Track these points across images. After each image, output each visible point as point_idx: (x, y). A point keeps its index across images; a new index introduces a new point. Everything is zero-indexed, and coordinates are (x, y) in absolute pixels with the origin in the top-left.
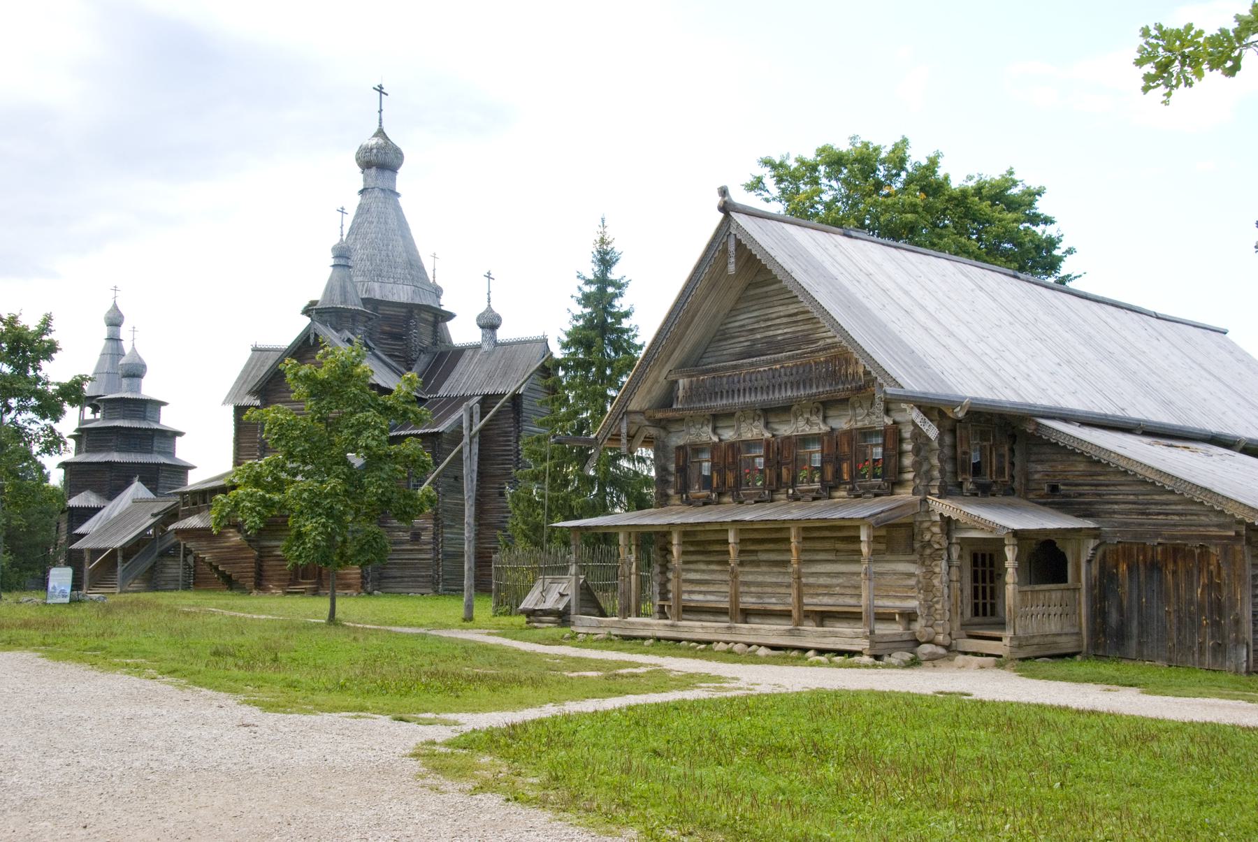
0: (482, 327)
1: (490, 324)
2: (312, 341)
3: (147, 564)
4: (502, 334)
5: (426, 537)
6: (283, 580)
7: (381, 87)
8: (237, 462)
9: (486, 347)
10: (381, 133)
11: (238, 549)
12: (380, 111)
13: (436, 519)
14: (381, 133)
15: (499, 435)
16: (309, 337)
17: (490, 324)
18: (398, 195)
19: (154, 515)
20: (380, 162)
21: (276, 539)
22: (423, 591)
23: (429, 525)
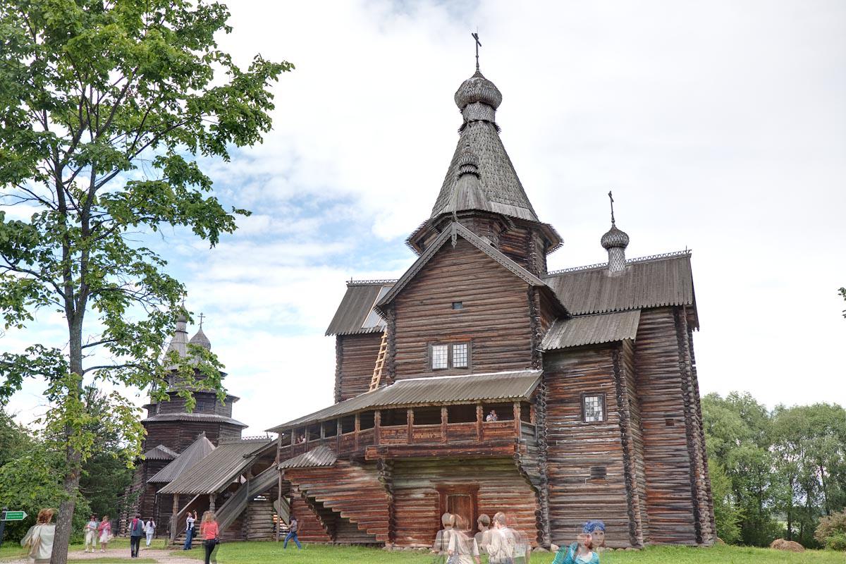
0: (608, 247)
1: (615, 242)
2: (454, 243)
3: (237, 511)
4: (633, 253)
5: (613, 473)
6: (426, 530)
7: (476, 35)
8: (340, 398)
9: (618, 267)
10: (478, 74)
11: (367, 490)
12: (477, 57)
13: (626, 450)
14: (478, 74)
15: (659, 355)
16: (450, 240)
17: (615, 242)
18: (497, 128)
19: (246, 457)
20: (479, 99)
21: (414, 479)
22: (616, 543)
23: (618, 457)
